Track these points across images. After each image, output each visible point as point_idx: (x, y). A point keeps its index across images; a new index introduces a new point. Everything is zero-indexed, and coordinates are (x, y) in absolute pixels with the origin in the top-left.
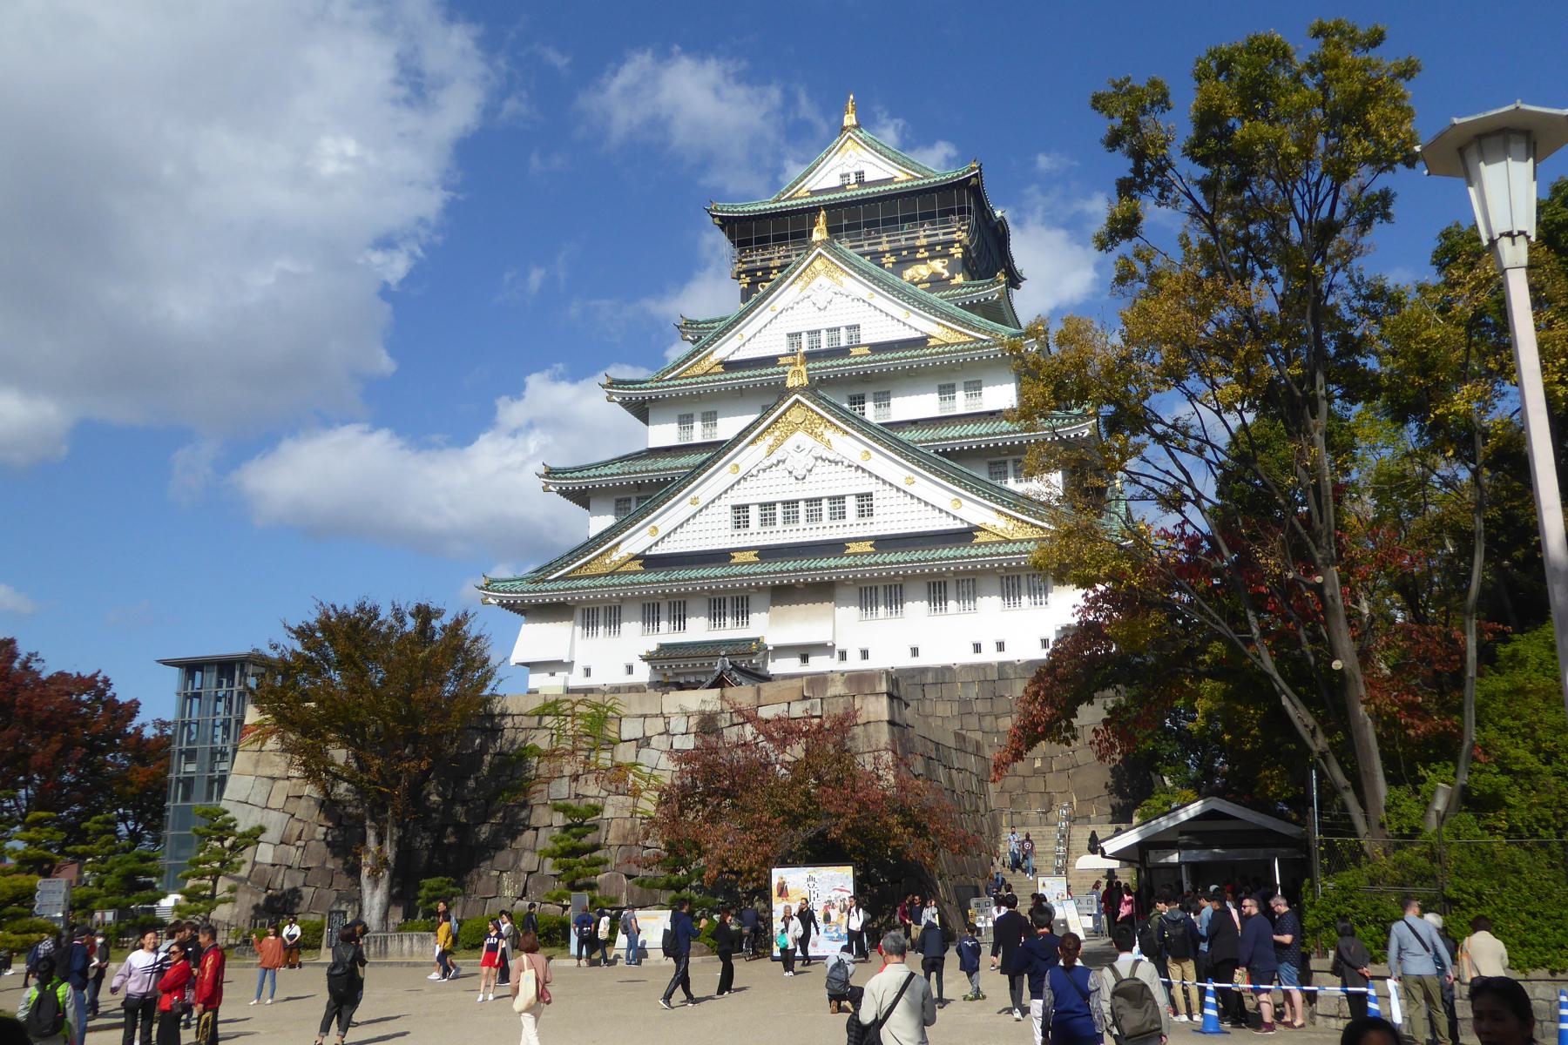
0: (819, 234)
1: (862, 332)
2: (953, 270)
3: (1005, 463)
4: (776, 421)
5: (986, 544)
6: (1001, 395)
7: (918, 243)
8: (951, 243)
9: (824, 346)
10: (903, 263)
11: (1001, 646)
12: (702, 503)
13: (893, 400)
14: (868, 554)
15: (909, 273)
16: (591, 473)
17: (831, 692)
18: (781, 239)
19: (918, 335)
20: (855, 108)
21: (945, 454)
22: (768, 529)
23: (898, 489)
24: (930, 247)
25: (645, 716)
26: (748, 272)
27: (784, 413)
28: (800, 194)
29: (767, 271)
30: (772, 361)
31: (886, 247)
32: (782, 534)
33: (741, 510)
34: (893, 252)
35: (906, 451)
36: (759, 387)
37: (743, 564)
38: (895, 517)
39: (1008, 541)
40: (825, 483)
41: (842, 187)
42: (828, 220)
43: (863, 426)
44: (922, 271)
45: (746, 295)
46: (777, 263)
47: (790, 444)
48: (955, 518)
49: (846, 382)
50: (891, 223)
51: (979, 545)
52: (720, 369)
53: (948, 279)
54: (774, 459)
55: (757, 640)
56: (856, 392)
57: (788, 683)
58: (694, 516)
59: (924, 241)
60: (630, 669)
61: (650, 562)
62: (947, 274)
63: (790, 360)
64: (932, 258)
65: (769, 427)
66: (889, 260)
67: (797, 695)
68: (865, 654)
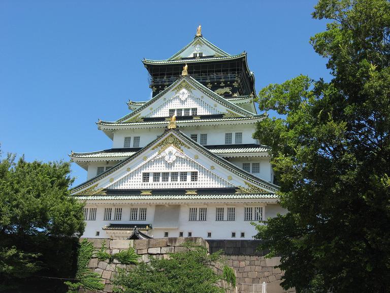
1: (198, 111)
3: (249, 164)
7: (221, 80)
8: (233, 82)
9: (183, 115)
11: (243, 235)
12: (132, 171)
14: (196, 195)
16: (89, 156)
17: (177, 244)
18: (169, 75)
21: (227, 158)
26: (156, 86)
29: (163, 87)
30: (163, 119)
31: (209, 81)
32: (161, 185)
40: (179, 168)
41: (194, 58)
42: (188, 69)
44: (223, 91)
45: (154, 94)
46: (168, 83)
47: (167, 151)
54: (160, 157)
55: (148, 225)
56: (194, 133)
59: (223, 80)
60: (98, 234)
61: (110, 192)
62: (231, 93)
64: (226, 86)
66: (210, 85)
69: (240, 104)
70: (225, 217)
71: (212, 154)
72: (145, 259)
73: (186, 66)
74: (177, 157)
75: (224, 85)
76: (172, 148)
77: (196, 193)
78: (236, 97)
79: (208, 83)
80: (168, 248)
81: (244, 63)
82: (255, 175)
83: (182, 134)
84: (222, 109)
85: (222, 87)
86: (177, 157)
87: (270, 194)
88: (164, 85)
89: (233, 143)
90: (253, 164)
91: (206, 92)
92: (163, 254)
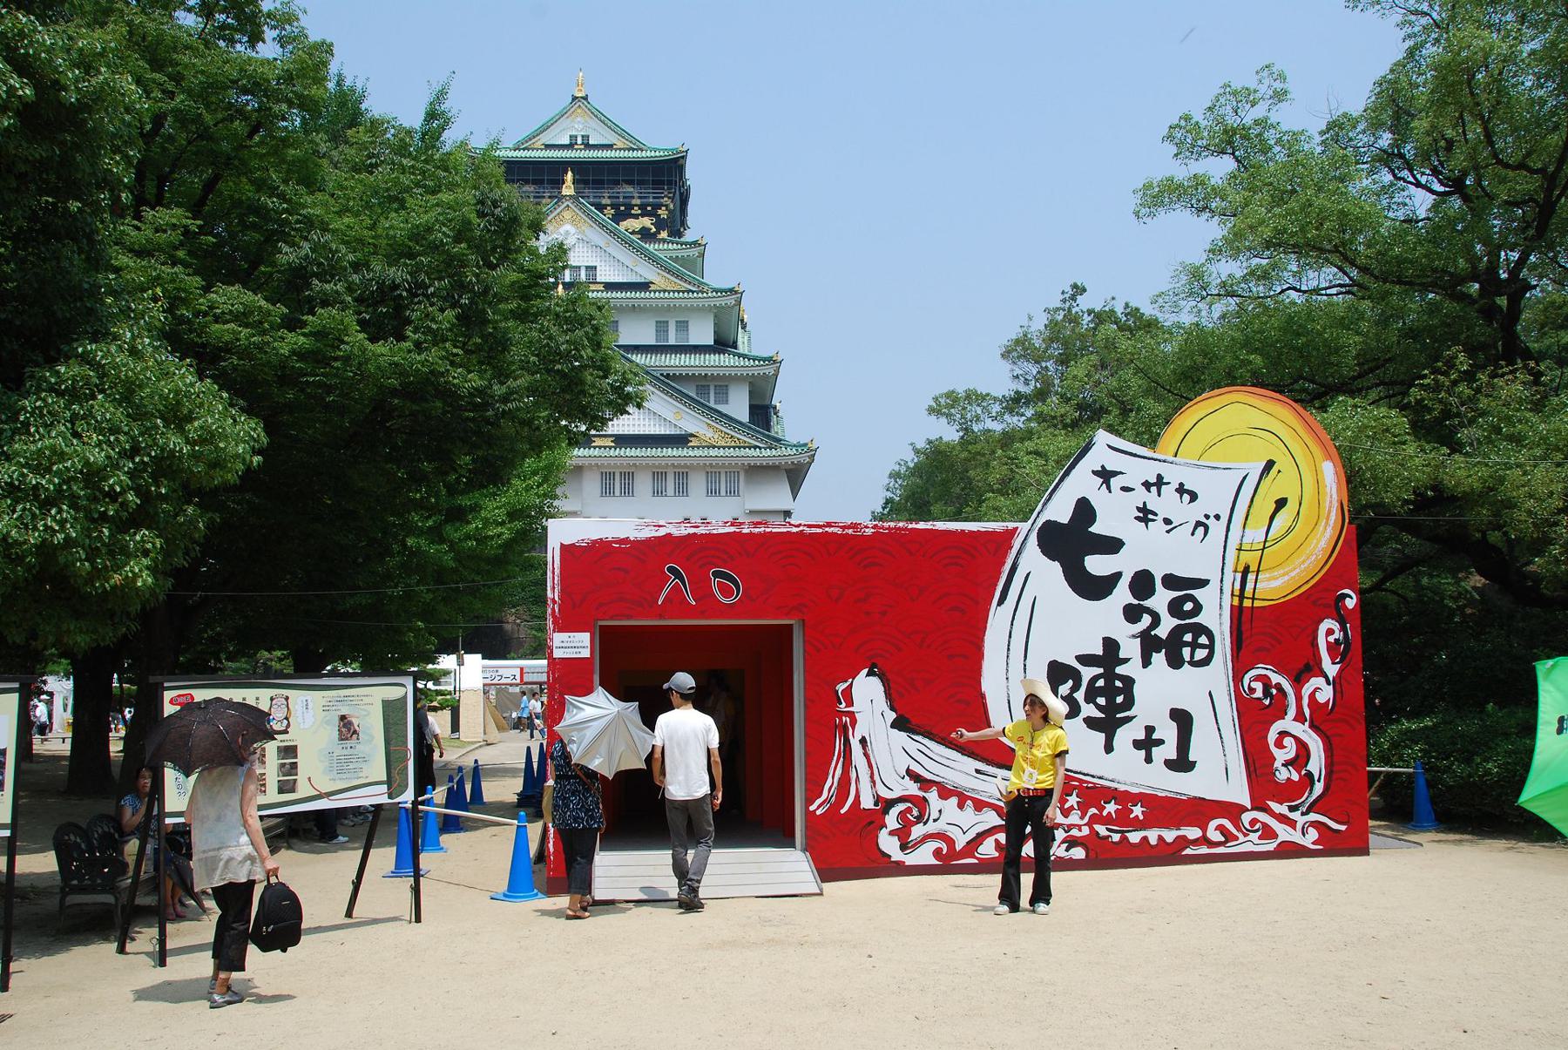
0: (568, 189)
2: (660, 225)
6: (703, 334)
7: (634, 202)
8: (659, 206)
10: (618, 218)
15: (624, 225)
21: (668, 376)
28: (538, 145)
41: (570, 146)
59: (638, 202)
66: (610, 211)
69: (676, 260)
70: (670, 490)
73: (570, 175)
78: (664, 241)
79: (605, 207)
81: (681, 169)
82: (720, 407)
84: (647, 272)
85: (636, 217)
87: (755, 447)
89: (672, 342)
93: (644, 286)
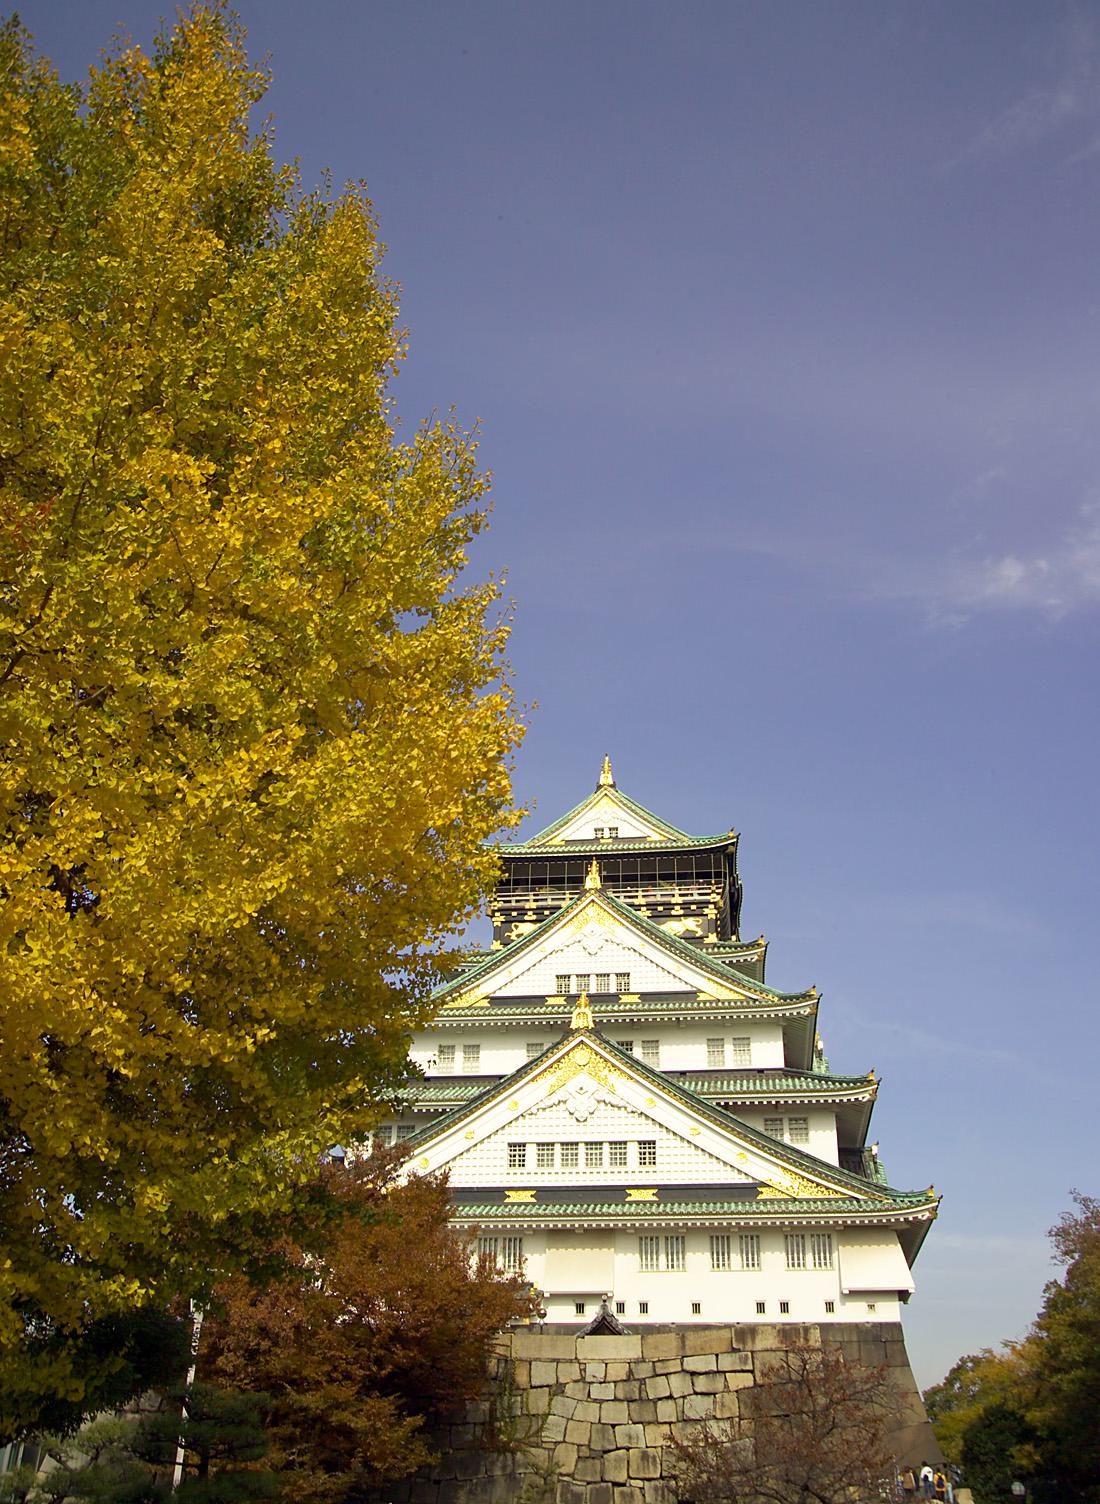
0: (593, 880)
3: (781, 1120)
4: (559, 1061)
5: (772, 1201)
6: (768, 1052)
9: (593, 990)
11: (784, 1307)
13: (661, 1047)
14: (652, 1203)
17: (760, 1345)
19: (688, 988)
20: (611, 769)
22: (546, 1170)
23: (682, 1139)
24: (685, 905)
25: (558, 1361)
27: (567, 1053)
28: (556, 841)
29: (523, 911)
33: (518, 1147)
34: (647, 905)
35: (693, 1101)
36: (541, 1027)
37: (520, 1204)
38: (678, 1166)
39: (795, 1200)
43: (648, 1072)
47: (572, 1086)
48: (740, 1171)
49: (626, 1027)
50: (650, 879)
51: (765, 1202)
52: (485, 1003)
53: (701, 938)
54: (554, 1099)
55: (532, 1285)
57: (714, 1333)
58: (468, 1150)
59: (680, 900)
63: (561, 1001)
65: (551, 1066)
67: (725, 1347)
68: (644, 1308)
71: (691, 1097)
72: (678, 1385)
74: (598, 1102)
75: (682, 912)
76: (583, 1079)
77: (655, 1198)
80: (737, 1355)
81: (731, 859)
83: (608, 1042)
86: (598, 1102)
88: (523, 909)
89: (729, 1065)
90: (791, 1120)
91: (652, 933)
92: (725, 1372)
93: (691, 995)
